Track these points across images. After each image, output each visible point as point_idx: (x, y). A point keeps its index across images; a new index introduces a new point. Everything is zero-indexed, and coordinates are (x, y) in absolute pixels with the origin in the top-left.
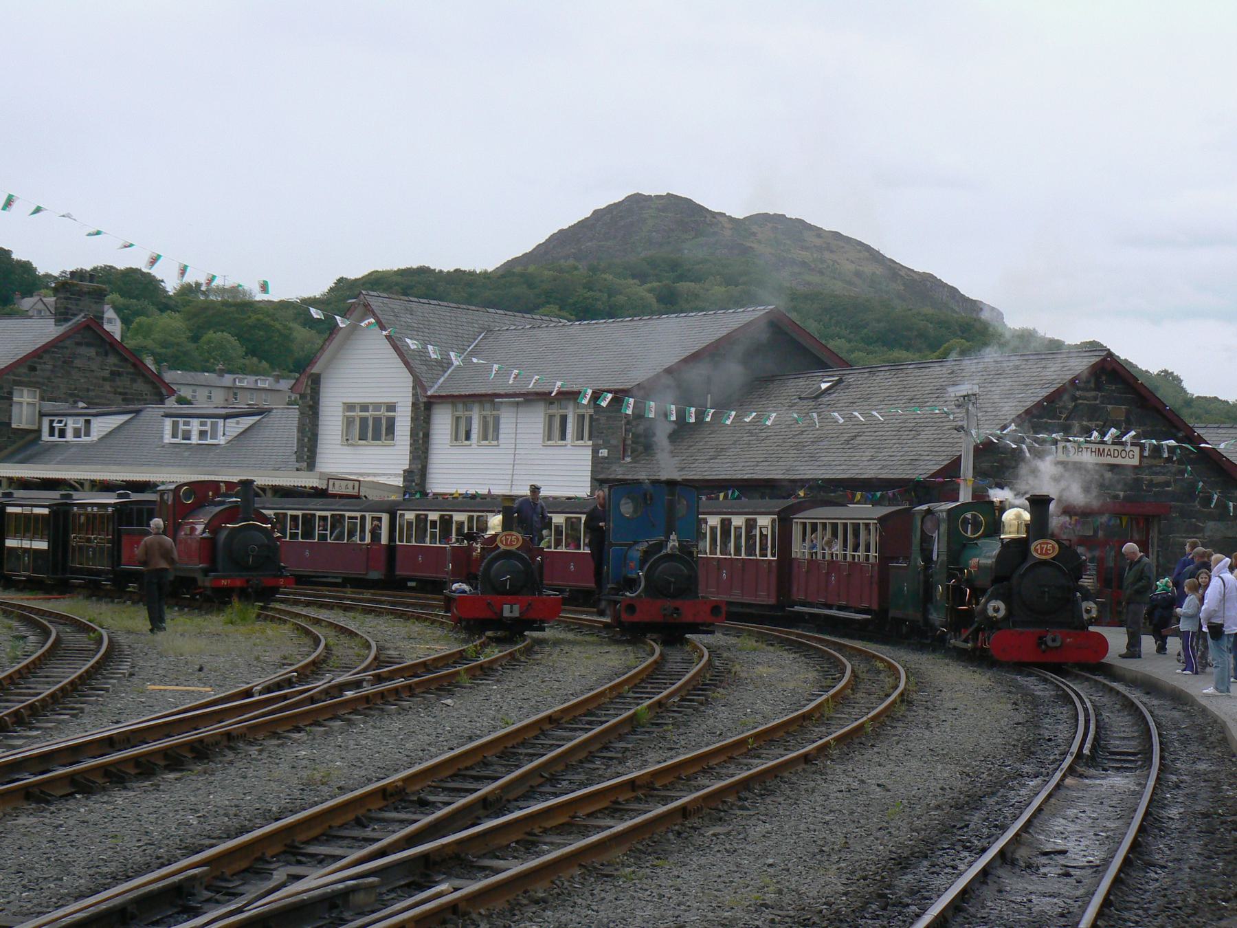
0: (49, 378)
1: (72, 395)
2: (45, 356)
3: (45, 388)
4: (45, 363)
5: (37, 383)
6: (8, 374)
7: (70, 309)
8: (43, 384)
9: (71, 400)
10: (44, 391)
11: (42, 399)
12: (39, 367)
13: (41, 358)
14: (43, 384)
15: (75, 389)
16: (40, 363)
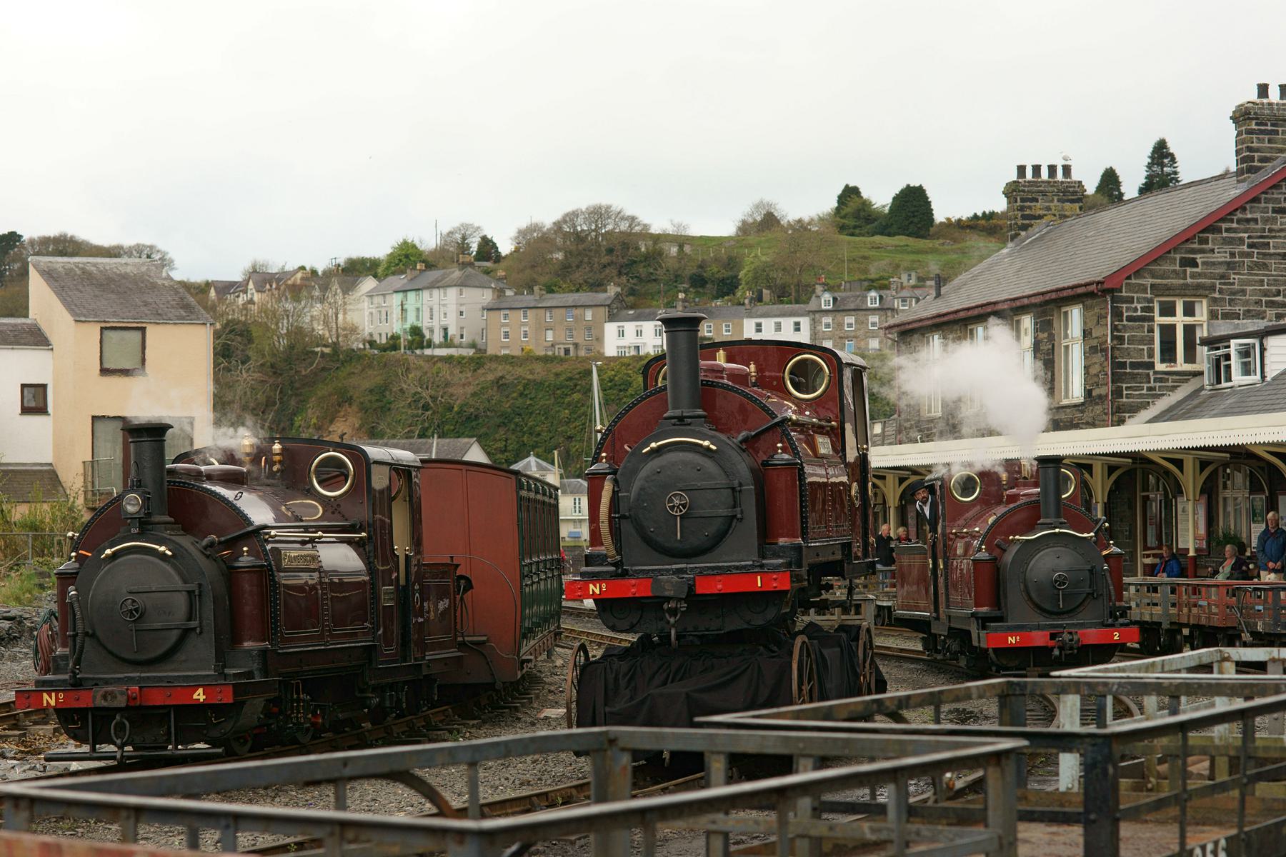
0: (1222, 277)
1: (1271, 304)
2: (1210, 236)
3: (1217, 295)
4: (1212, 251)
5: (1199, 286)
6: (1138, 274)
7: (1257, 150)
8: (1212, 288)
9: (1271, 312)
10: (1215, 300)
11: (1213, 315)
12: (1199, 258)
13: (1206, 241)
14: (1212, 288)
15: (1278, 293)
16: (1202, 251)
